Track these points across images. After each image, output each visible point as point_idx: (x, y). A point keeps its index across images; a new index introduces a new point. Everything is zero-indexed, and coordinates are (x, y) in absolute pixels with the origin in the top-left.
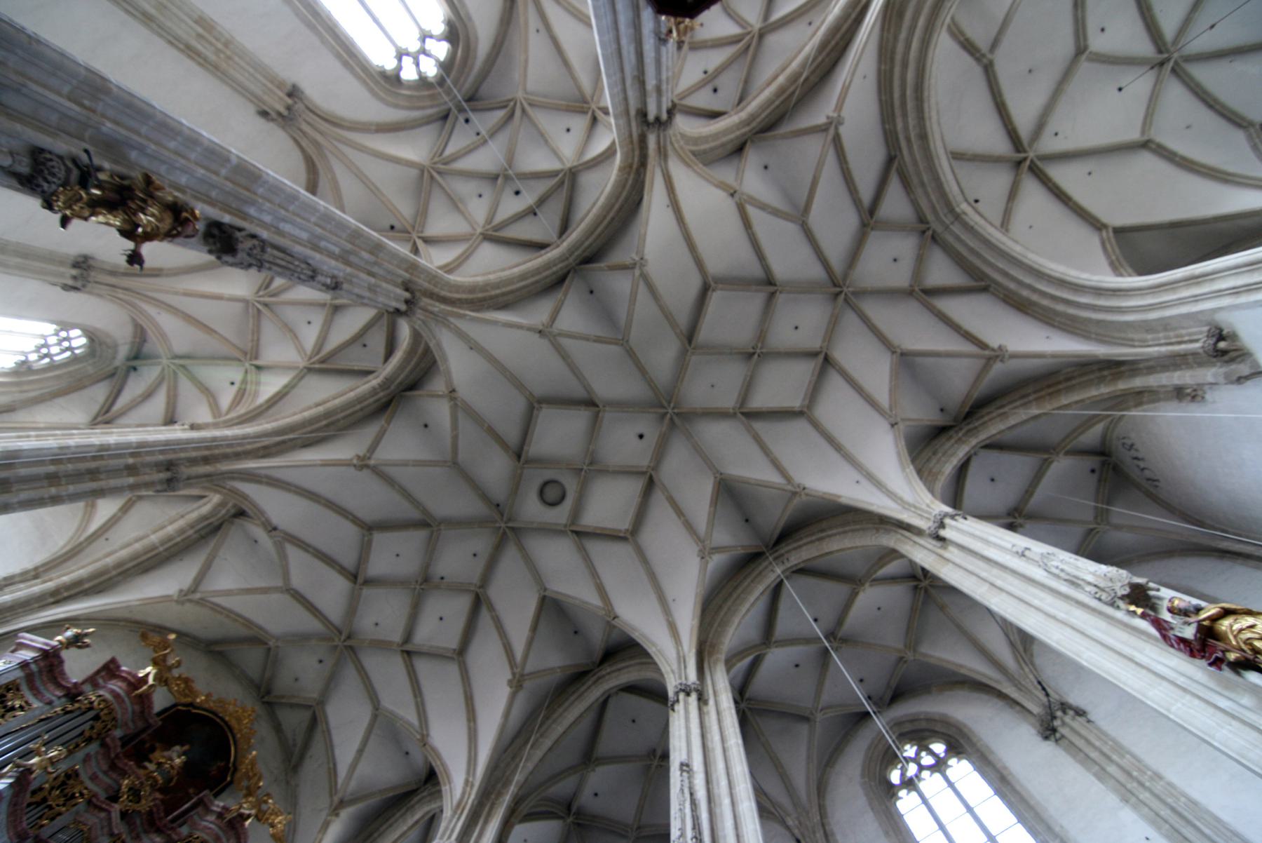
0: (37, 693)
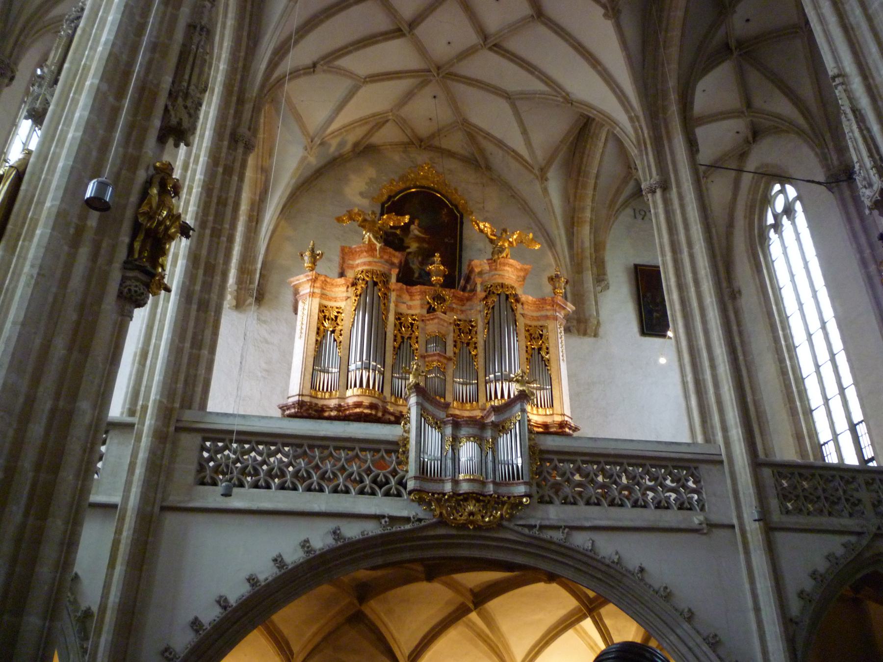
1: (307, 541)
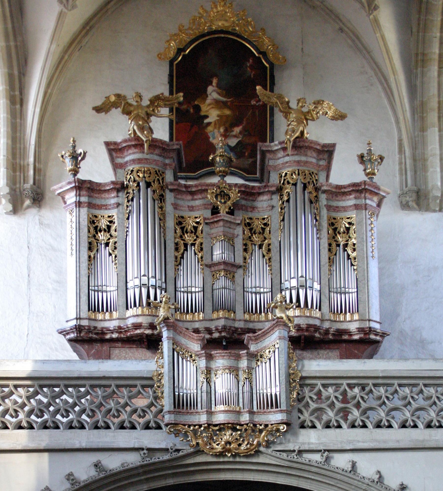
0: (105, 207)
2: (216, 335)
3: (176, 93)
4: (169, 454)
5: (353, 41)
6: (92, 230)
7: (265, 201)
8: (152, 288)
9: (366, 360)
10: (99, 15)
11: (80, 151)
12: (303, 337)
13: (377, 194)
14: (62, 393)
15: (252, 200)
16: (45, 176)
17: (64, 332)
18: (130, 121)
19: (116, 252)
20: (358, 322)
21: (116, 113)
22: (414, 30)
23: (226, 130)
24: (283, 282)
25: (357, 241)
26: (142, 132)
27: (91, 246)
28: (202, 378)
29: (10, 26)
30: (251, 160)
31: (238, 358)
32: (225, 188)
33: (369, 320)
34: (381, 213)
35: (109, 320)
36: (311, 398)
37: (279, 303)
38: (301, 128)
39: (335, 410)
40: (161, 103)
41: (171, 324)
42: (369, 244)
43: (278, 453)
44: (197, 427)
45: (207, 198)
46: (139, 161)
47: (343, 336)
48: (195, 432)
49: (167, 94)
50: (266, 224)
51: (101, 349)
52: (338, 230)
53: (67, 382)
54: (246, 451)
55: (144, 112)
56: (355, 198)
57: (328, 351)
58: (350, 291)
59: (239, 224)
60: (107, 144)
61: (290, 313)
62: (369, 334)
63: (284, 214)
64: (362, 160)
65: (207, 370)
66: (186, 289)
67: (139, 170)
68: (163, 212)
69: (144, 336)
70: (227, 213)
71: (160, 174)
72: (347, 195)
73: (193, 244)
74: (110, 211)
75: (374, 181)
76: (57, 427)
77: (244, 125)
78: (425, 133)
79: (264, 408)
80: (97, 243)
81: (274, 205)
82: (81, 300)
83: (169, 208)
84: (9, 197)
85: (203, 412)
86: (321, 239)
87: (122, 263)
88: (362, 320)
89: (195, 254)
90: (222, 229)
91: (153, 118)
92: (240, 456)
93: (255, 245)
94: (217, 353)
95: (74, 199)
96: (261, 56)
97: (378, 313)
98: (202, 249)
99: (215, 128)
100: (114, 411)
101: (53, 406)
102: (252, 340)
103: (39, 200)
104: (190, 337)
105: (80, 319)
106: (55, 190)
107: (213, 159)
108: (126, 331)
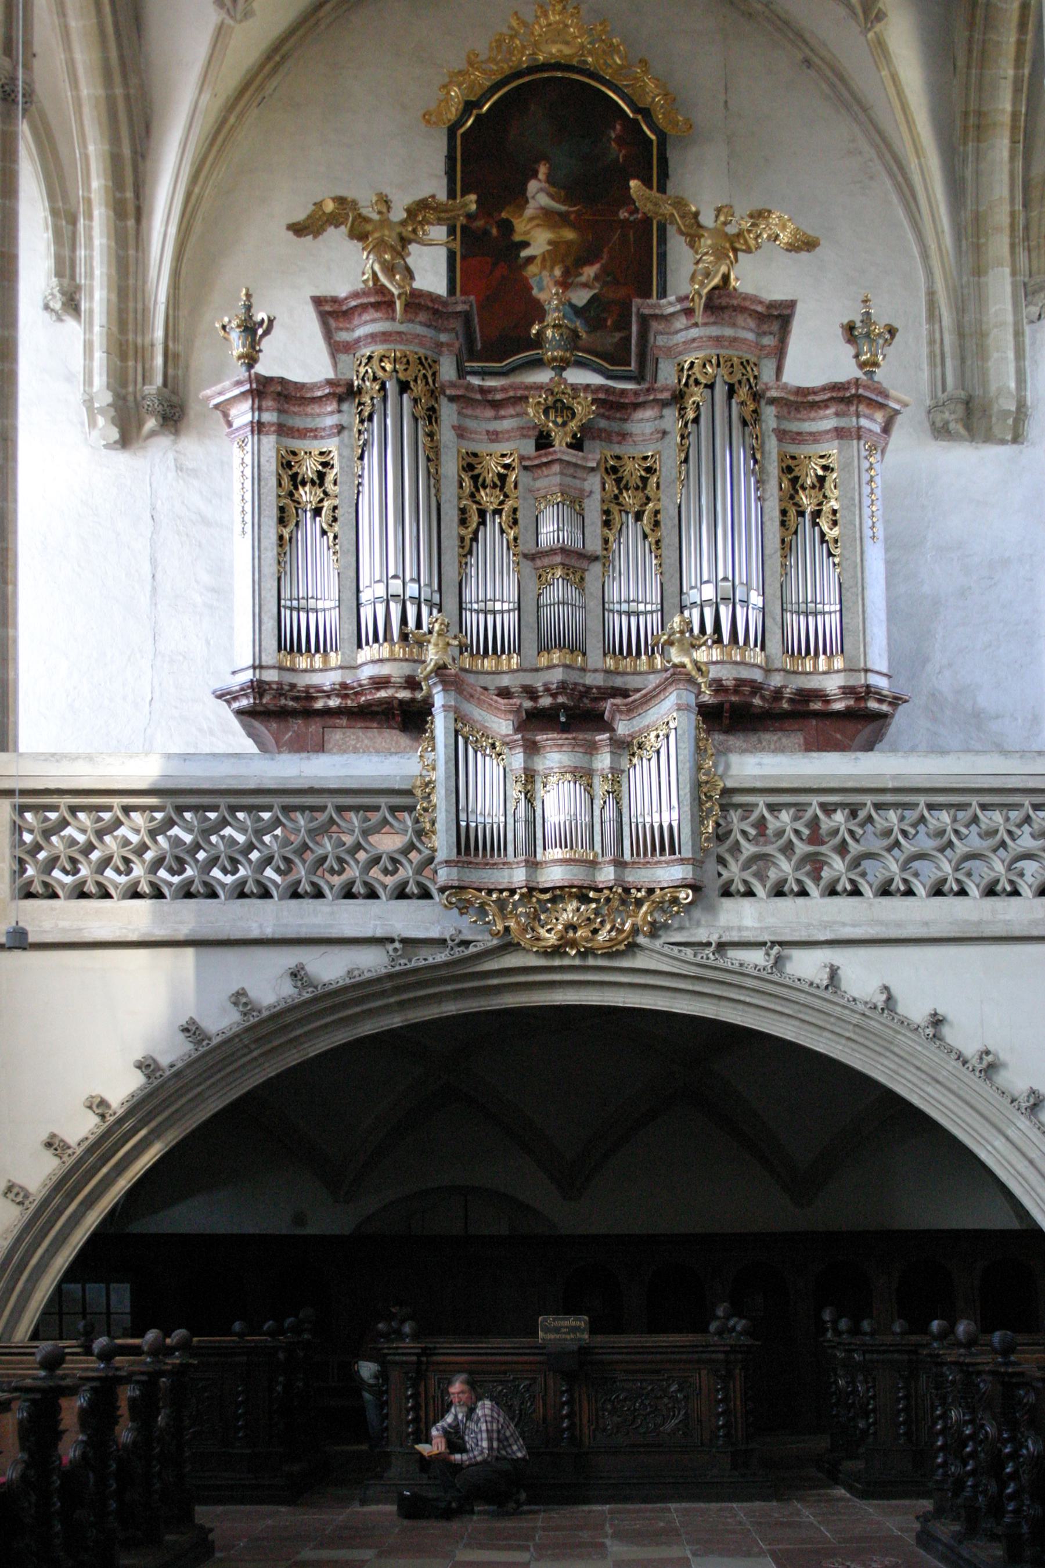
0: (314, 433)
1: (241, 993)
2: (546, 702)
3: (462, 196)
4: (448, 950)
5: (832, 86)
6: (286, 481)
7: (648, 420)
8: (412, 604)
9: (860, 754)
10: (300, 33)
11: (260, 315)
12: (727, 706)
13: (882, 406)
14: (224, 823)
15: (621, 419)
16: (187, 367)
17: (226, 696)
18: (365, 253)
19: (336, 527)
20: (843, 674)
21: (336, 237)
22: (961, 63)
23: (566, 273)
24: (685, 590)
25: (841, 505)
26: (391, 276)
27: (285, 515)
28: (515, 791)
29: (114, 54)
30: (618, 335)
31: (592, 749)
32: (563, 393)
33: (867, 671)
34: (890, 447)
35: (321, 670)
36: (744, 833)
37: (678, 635)
38: (723, 269)
39: (795, 859)
40: (430, 216)
41: (452, 679)
42: (867, 512)
43: (676, 948)
44: (505, 894)
45: (527, 414)
46: (385, 337)
47: (811, 704)
48: (501, 904)
49: (442, 196)
50: (649, 470)
51: (304, 730)
52: (800, 482)
53: (233, 801)
54: (608, 944)
55: (394, 235)
56: (837, 414)
57: (780, 734)
58: (827, 608)
59: (593, 469)
60: (318, 301)
61: (701, 655)
62: (864, 699)
63: (688, 448)
64: (851, 334)
65: (526, 776)
66: (482, 605)
67: (384, 356)
68: (435, 445)
69: (395, 703)
70: (570, 446)
71: (428, 364)
72: (819, 408)
73: (498, 512)
74: (323, 441)
75: (876, 378)
76: (213, 895)
77: (603, 261)
78: (983, 280)
79: (645, 854)
80: (297, 509)
81: (668, 430)
82: (263, 628)
83: (446, 435)
84: (112, 412)
85: (517, 863)
86: (764, 500)
87: (348, 550)
88: (851, 670)
89: (502, 531)
90: (557, 479)
91: (413, 248)
92: (595, 956)
93: (627, 513)
94: (547, 740)
95: (248, 417)
96: (639, 117)
97: (885, 656)
98: (515, 522)
99: (544, 267)
100: (331, 861)
101: (205, 850)
102: (621, 712)
103: (175, 418)
104: (491, 705)
105: (261, 667)
106: (209, 398)
107: (540, 333)
108: (356, 694)
